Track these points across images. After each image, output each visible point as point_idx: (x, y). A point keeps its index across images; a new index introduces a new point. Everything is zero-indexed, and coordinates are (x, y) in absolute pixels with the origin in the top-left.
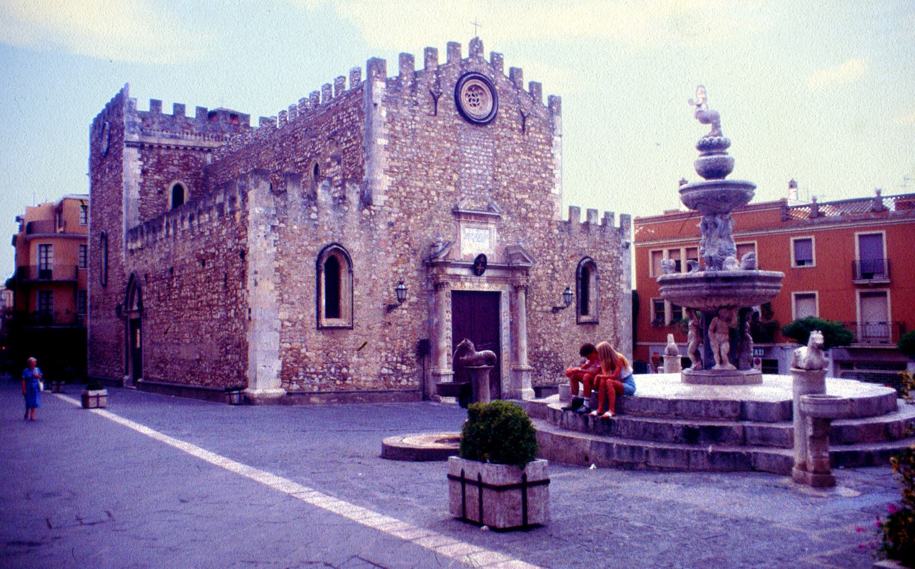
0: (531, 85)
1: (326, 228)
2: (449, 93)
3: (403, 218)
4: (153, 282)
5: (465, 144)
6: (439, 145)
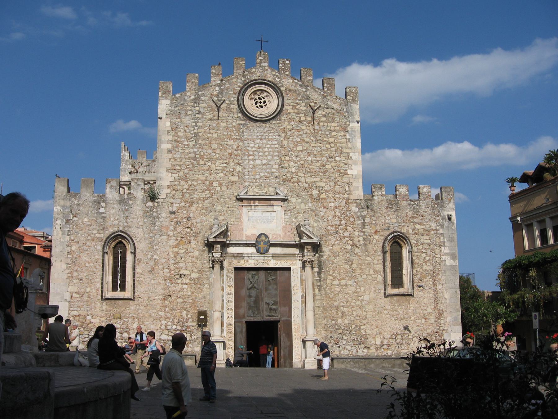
1: (112, 219)
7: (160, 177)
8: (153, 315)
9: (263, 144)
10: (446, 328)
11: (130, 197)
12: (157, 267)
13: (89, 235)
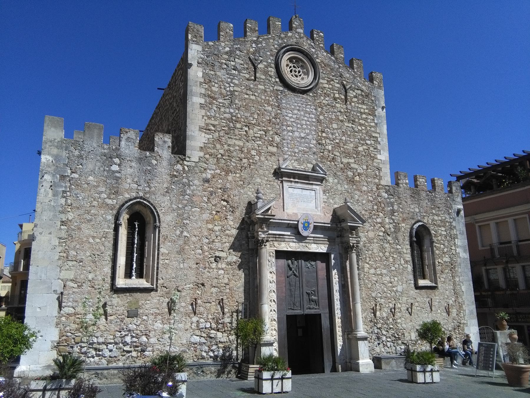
1: (129, 181)
5: (287, 108)
7: (191, 135)
9: (301, 115)
10: (465, 322)
12: (187, 247)
13: (94, 200)
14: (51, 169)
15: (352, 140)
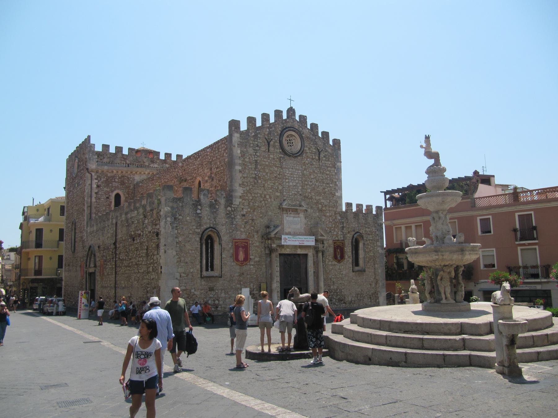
0: (323, 133)
2: (276, 139)
3: (250, 211)
4: (103, 250)
5: (285, 168)
6: (271, 169)
8: (233, 287)
9: (293, 171)
10: (379, 290)
11: (217, 203)
14: (170, 215)
15: (322, 185)
